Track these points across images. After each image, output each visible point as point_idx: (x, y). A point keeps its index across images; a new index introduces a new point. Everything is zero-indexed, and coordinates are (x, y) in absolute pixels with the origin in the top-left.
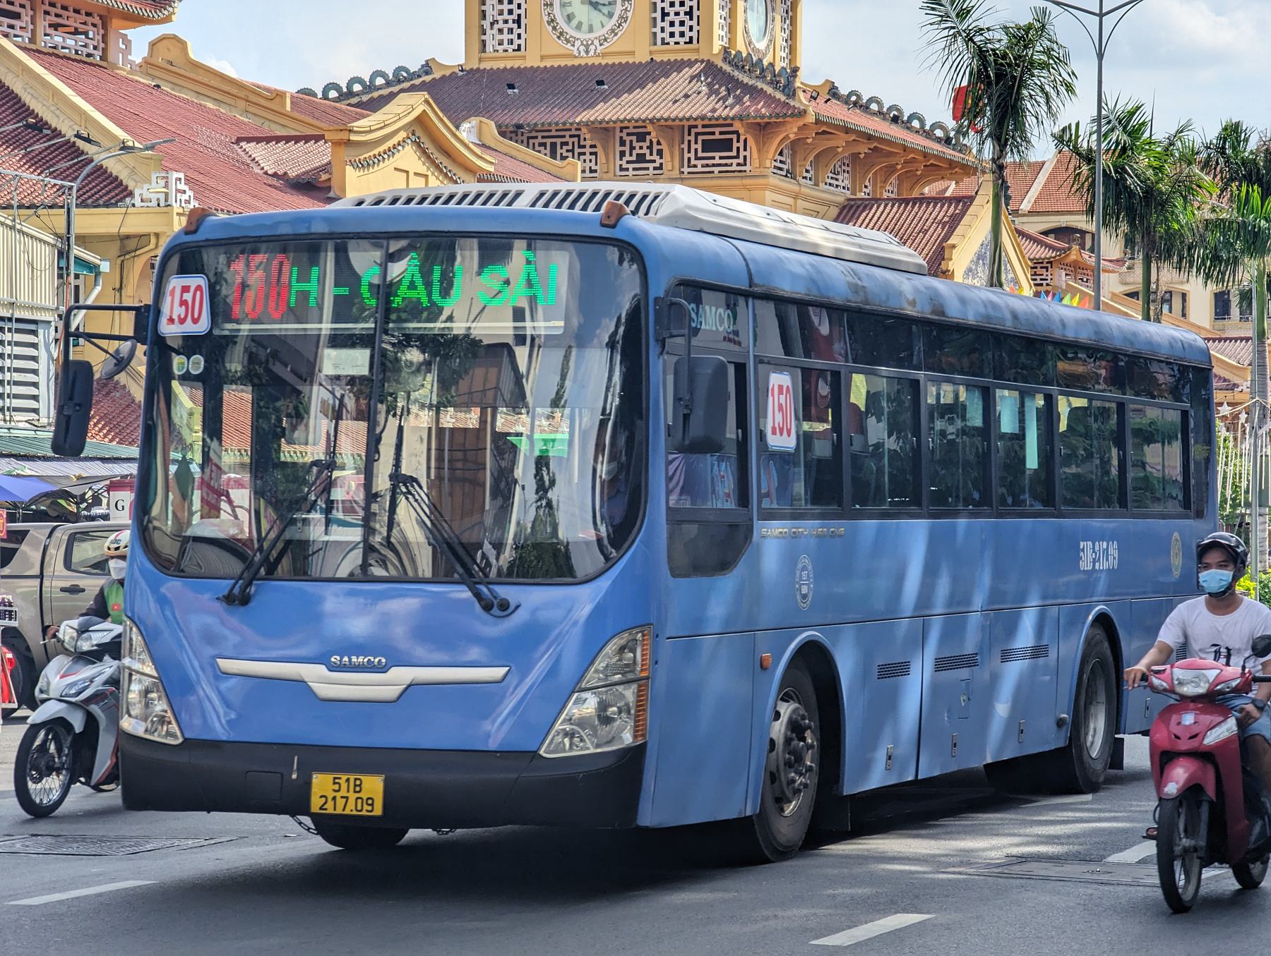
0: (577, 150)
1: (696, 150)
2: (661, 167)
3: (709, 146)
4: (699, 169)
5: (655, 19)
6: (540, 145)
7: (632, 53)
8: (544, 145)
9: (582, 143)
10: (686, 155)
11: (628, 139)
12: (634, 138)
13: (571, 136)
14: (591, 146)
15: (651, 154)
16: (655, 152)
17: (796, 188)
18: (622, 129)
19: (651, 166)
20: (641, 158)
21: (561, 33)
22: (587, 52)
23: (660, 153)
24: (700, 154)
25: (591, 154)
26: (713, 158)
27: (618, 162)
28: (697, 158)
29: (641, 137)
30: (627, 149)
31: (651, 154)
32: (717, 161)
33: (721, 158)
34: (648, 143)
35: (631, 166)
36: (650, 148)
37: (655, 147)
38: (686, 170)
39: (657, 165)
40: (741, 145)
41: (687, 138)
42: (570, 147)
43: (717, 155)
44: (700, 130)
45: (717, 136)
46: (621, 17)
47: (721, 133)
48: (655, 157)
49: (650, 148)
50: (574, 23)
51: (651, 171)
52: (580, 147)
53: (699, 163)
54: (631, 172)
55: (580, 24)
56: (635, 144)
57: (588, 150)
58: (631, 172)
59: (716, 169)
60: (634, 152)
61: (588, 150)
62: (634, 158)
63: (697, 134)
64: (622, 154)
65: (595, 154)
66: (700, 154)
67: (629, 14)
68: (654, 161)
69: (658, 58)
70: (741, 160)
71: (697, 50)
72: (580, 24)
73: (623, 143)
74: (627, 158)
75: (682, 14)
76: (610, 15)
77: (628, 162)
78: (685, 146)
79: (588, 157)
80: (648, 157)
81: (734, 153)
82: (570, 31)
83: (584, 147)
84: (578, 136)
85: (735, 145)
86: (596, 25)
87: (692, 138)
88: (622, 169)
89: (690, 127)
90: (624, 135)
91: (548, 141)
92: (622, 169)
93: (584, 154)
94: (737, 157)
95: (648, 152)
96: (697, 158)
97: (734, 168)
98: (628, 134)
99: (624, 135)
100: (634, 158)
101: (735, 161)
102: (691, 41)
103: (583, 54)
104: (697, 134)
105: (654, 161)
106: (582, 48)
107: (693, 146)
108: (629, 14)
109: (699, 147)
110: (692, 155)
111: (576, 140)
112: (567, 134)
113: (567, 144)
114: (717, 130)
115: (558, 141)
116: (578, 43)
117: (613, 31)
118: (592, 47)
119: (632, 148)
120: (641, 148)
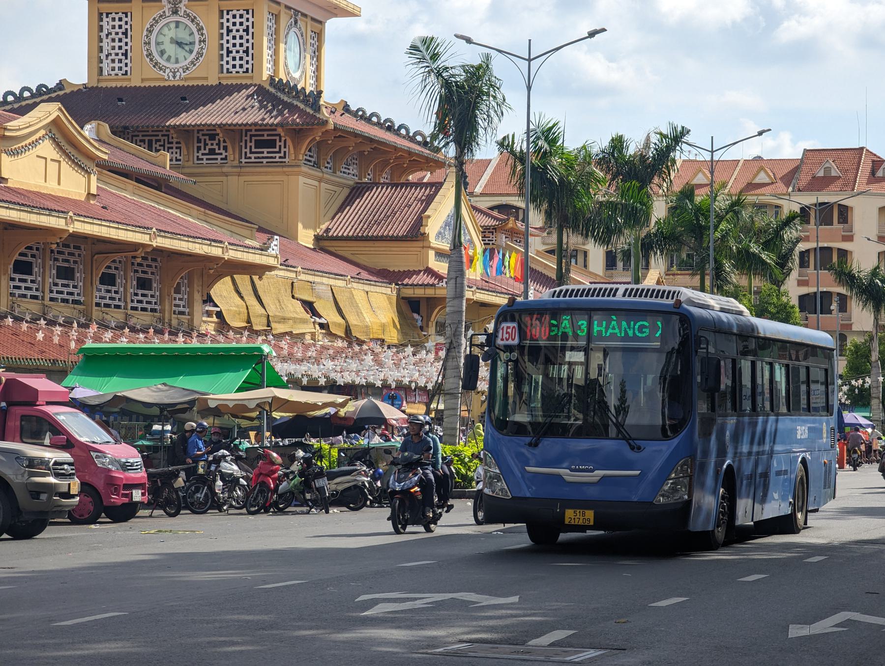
0: (167, 145)
1: (251, 147)
2: (226, 158)
3: (260, 144)
4: (253, 160)
5: (222, 55)
6: (141, 141)
7: (206, 78)
8: (143, 141)
9: (170, 140)
10: (244, 150)
11: (203, 138)
12: (207, 138)
13: (163, 135)
14: (177, 143)
15: (219, 149)
17: (320, 174)
18: (198, 131)
19: (219, 157)
20: (212, 152)
21: (156, 63)
22: (174, 77)
23: (225, 148)
24: (253, 150)
25: (177, 148)
26: (263, 153)
27: (196, 154)
29: (212, 137)
30: (202, 145)
31: (219, 149)
32: (265, 155)
33: (268, 153)
35: (205, 157)
36: (218, 144)
37: (222, 144)
38: (243, 160)
39: (223, 156)
40: (282, 144)
41: (244, 138)
42: (162, 143)
43: (265, 150)
44: (253, 133)
45: (266, 138)
46: (198, 53)
47: (268, 135)
49: (218, 144)
50: (165, 56)
51: (219, 161)
52: (169, 143)
53: (253, 156)
54: (205, 162)
55: (169, 57)
56: (207, 141)
57: (174, 145)
58: (205, 162)
59: (265, 161)
60: (207, 148)
61: (174, 145)
62: (207, 151)
63: (251, 136)
64: (199, 149)
65: (180, 148)
66: (253, 150)
67: (204, 51)
68: (221, 154)
69: (224, 82)
70: (282, 155)
71: (252, 78)
72: (169, 57)
73: (199, 141)
74: (202, 151)
75: (241, 52)
76: (191, 52)
77: (203, 154)
78: (243, 144)
79: (174, 150)
80: (217, 151)
81: (277, 149)
82: (162, 62)
83: (172, 143)
84: (168, 136)
85: (278, 144)
86: (181, 59)
87: (248, 138)
88: (198, 159)
89: (247, 131)
90: (200, 135)
91: (147, 139)
92: (198, 159)
93: (172, 148)
94: (279, 152)
95: (217, 147)
96: (251, 152)
97: (277, 159)
98: (203, 135)
99: (200, 135)
100: (207, 151)
101: (278, 155)
102: (247, 71)
103: (171, 78)
104: (251, 136)
105: (221, 154)
106: (171, 74)
107: (249, 144)
108: (204, 51)
109: (253, 144)
110: (248, 150)
111: (166, 138)
112: (160, 134)
113: (160, 141)
114: (266, 133)
115: (154, 138)
116: (168, 71)
117: (192, 62)
118: (178, 74)
119: (206, 145)
120: (212, 144)
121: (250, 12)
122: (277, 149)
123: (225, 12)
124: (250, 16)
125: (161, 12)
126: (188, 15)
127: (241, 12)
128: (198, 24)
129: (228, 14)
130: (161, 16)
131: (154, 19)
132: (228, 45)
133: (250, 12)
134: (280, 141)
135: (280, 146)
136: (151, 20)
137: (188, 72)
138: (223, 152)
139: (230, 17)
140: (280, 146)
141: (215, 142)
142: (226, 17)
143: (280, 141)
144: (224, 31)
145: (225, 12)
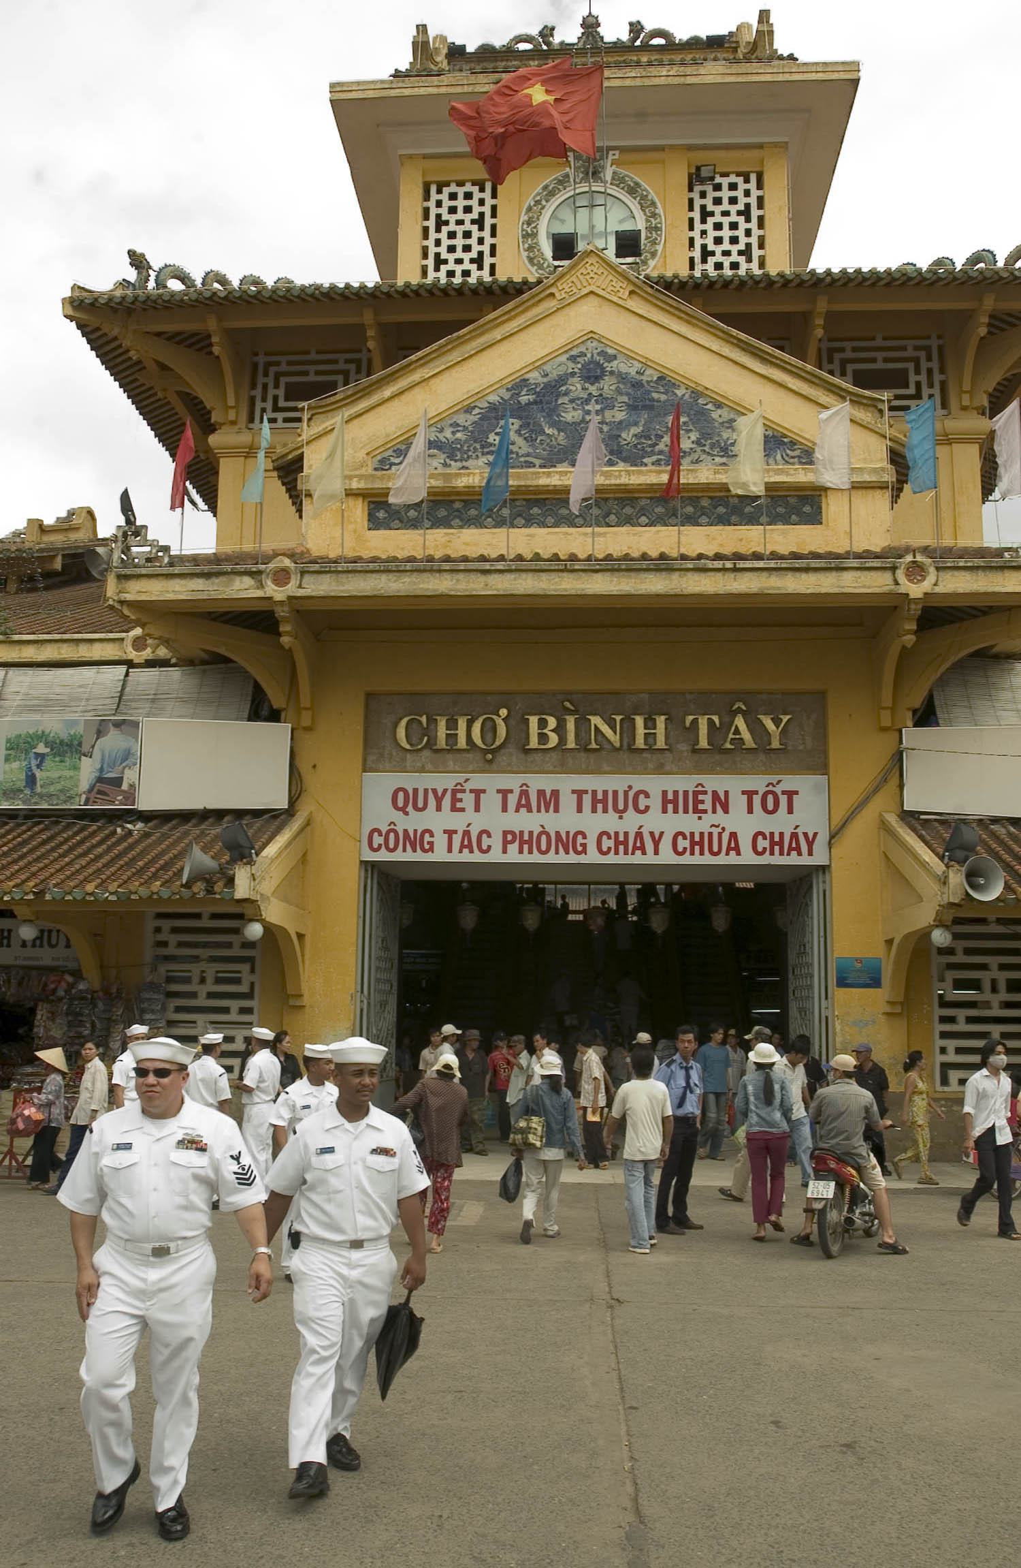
40: (923, 378)
45: (880, 365)
47: (886, 360)
81: (912, 390)
85: (913, 378)
121: (753, 177)
124: (752, 185)
125: (558, 174)
127: (733, 179)
128: (644, 198)
130: (560, 182)
131: (545, 187)
133: (753, 177)
134: (918, 372)
135: (918, 384)
136: (539, 189)
140: (918, 384)
143: (918, 372)
144: (696, 215)
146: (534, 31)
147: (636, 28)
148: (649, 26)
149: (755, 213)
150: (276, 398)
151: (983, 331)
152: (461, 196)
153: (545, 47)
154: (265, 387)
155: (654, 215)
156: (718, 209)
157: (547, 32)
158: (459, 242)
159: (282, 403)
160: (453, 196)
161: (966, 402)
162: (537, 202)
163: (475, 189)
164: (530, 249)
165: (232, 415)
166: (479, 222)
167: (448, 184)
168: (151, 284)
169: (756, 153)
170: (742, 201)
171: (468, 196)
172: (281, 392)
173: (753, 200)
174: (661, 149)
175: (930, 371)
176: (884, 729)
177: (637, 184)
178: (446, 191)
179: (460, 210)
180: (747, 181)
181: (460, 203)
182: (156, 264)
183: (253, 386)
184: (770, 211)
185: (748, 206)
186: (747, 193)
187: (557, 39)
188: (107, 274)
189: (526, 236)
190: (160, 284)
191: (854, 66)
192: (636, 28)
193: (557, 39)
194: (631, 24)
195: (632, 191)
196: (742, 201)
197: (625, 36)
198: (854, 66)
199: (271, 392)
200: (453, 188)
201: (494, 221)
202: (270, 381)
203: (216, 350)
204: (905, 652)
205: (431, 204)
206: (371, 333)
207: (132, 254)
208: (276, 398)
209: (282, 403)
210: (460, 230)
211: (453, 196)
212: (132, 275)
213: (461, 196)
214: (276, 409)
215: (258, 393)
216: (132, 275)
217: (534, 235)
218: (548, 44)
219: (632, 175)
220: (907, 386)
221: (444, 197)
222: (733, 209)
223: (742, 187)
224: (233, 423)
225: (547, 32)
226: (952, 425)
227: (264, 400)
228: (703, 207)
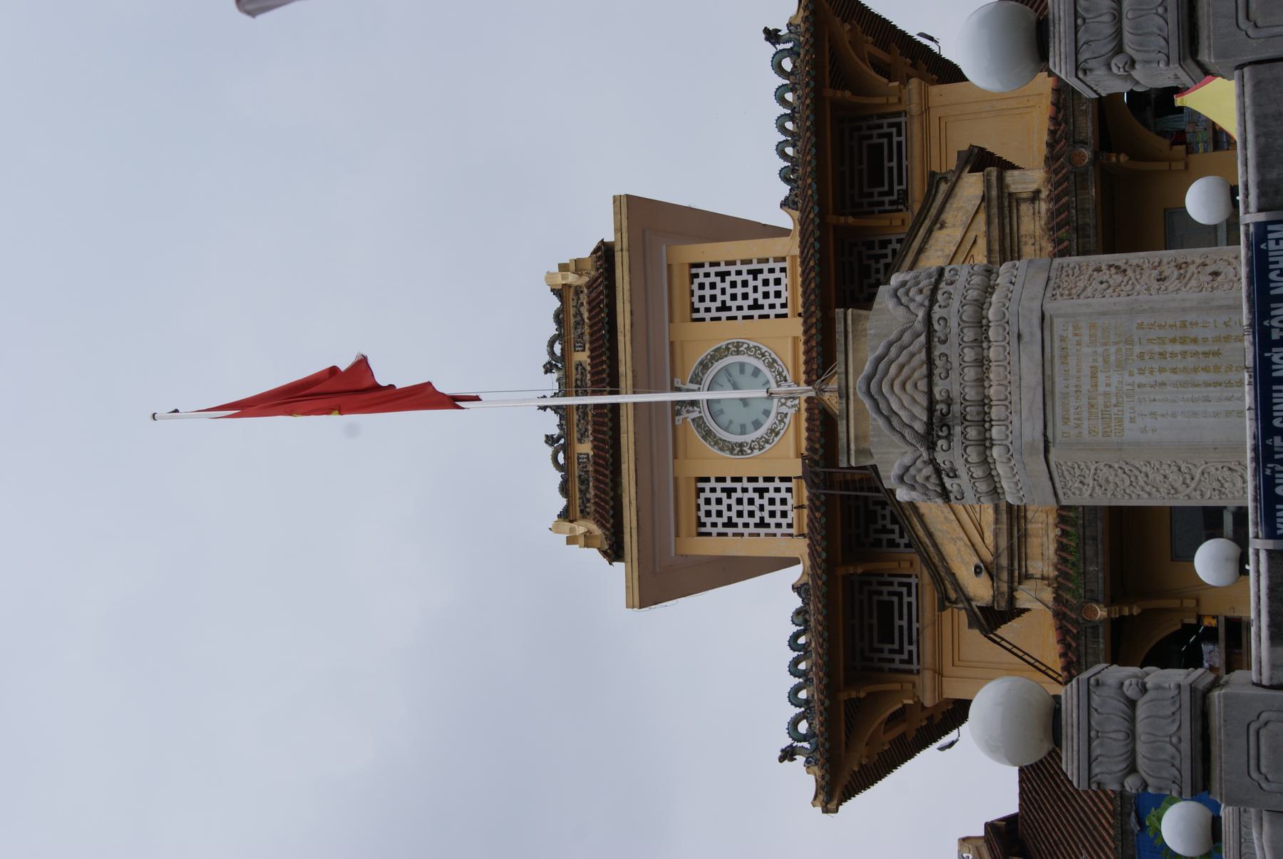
1: (881, 194)
7: (795, 339)
10: (887, 207)
16: (884, 251)
23: (884, 244)
24: (886, 188)
26: (891, 169)
28: (890, 192)
31: (885, 256)
32: (894, 164)
34: (872, 262)
37: (877, 251)
48: (889, 251)
49: (877, 258)
66: (886, 188)
71: (793, 257)
85: (876, 141)
87: (866, 200)
95: (883, 261)
96: (890, 192)
103: (796, 402)
106: (789, 403)
107: (876, 199)
110: (886, 199)
116: (784, 409)
121: (694, 271)
122: (885, 141)
123: (696, 316)
126: (695, 374)
127: (695, 287)
129: (697, 310)
130: (698, 426)
131: (704, 437)
132: (745, 308)
135: (880, 136)
137: (785, 373)
138: (890, 247)
139: (702, 306)
140: (880, 136)
141: (874, 266)
142: (702, 314)
144: (724, 315)
145: (696, 316)
146: (549, 450)
147: (548, 369)
148: (547, 358)
149: (723, 268)
150: (892, 651)
151: (848, 93)
152: (708, 508)
153: (562, 441)
154: (881, 660)
155: (727, 349)
156: (720, 298)
157: (550, 440)
158: (746, 508)
159: (896, 646)
160: (708, 514)
161: (896, 100)
162: (716, 443)
163: (703, 496)
164: (752, 449)
165: (910, 686)
166: (729, 492)
167: (699, 518)
168: (806, 745)
169: (676, 271)
170: (713, 279)
171: (708, 501)
172: (887, 647)
173: (713, 270)
174: (672, 343)
175: (869, 128)
176: (1187, 167)
177: (701, 363)
178: (703, 519)
179: (719, 508)
180: (697, 276)
181: (714, 508)
182: (790, 741)
183: (881, 670)
184: (721, 258)
185: (717, 274)
186: (707, 275)
187: (556, 431)
188: (801, 779)
189: (742, 452)
190: (804, 738)
191: (617, 199)
192: (548, 369)
193: (556, 431)
194: (546, 373)
195: (705, 366)
196: (713, 279)
197: (555, 376)
198: (617, 199)
199: (886, 655)
200: (702, 514)
201: (728, 480)
202: (877, 655)
203: (862, 695)
204: (1133, 157)
205: (714, 531)
206: (851, 570)
207: (782, 759)
208: (892, 651)
209: (896, 646)
210: (723, 507)
211: (708, 514)
212: (801, 759)
213: (708, 508)
214: (901, 651)
215: (887, 666)
216: (801, 759)
217: (741, 445)
218: (559, 438)
219: (693, 366)
220: (882, 144)
221: (708, 521)
222: (720, 285)
223: (701, 279)
224: (914, 686)
225: (550, 440)
226: (915, 108)
227: (893, 661)
228: (718, 309)
